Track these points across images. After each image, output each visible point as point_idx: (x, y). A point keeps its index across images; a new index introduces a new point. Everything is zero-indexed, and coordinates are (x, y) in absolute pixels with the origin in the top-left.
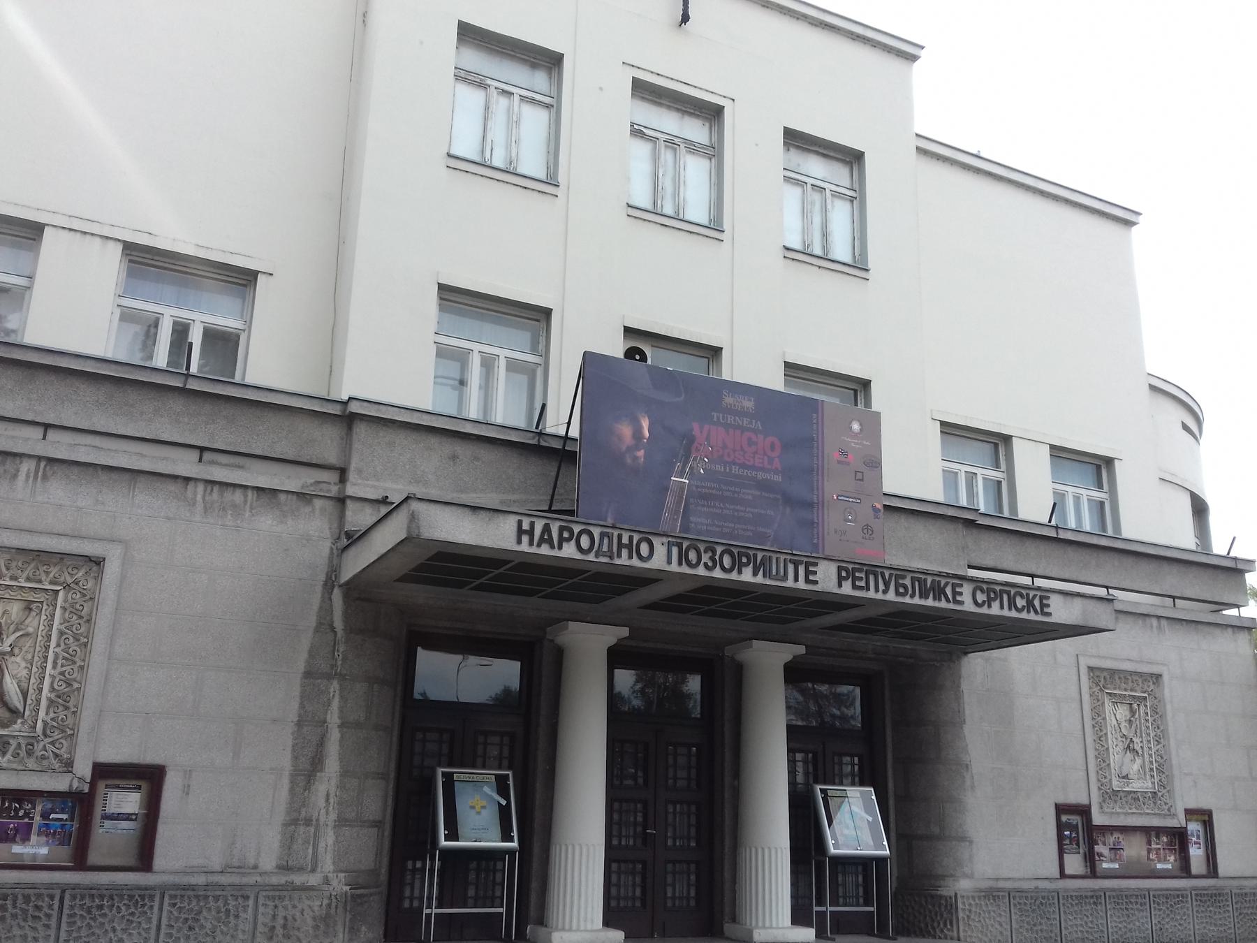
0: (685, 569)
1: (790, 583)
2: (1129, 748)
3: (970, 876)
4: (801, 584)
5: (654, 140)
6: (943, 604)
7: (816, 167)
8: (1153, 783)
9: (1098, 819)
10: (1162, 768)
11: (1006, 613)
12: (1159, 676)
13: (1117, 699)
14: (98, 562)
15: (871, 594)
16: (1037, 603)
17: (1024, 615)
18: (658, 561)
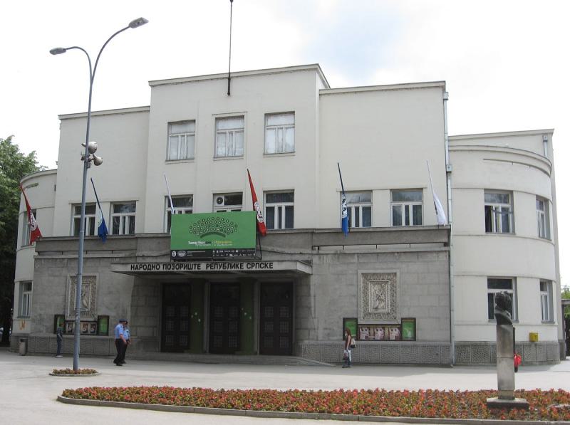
0: (168, 270)
1: (194, 270)
2: (379, 298)
4: (196, 270)
5: (225, 133)
6: (237, 269)
9: (360, 322)
10: (394, 304)
11: (257, 269)
12: (395, 273)
13: (375, 283)
14: (95, 277)
15: (216, 269)
16: (268, 265)
17: (264, 269)
18: (161, 269)
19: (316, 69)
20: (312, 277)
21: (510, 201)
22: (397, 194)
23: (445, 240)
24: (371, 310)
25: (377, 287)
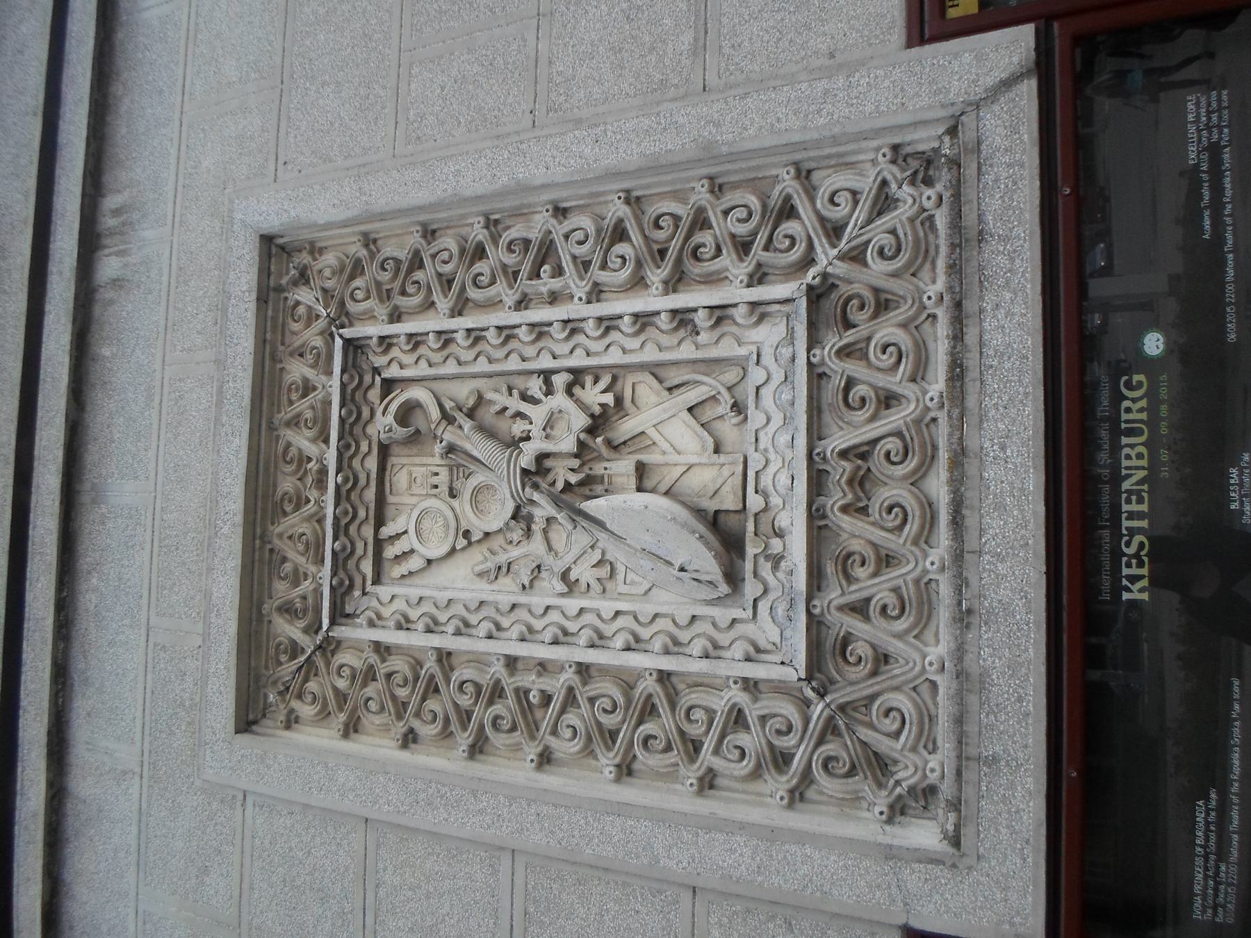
2: (567, 486)
12: (272, 247)
13: (363, 544)
24: (776, 634)
25: (421, 509)
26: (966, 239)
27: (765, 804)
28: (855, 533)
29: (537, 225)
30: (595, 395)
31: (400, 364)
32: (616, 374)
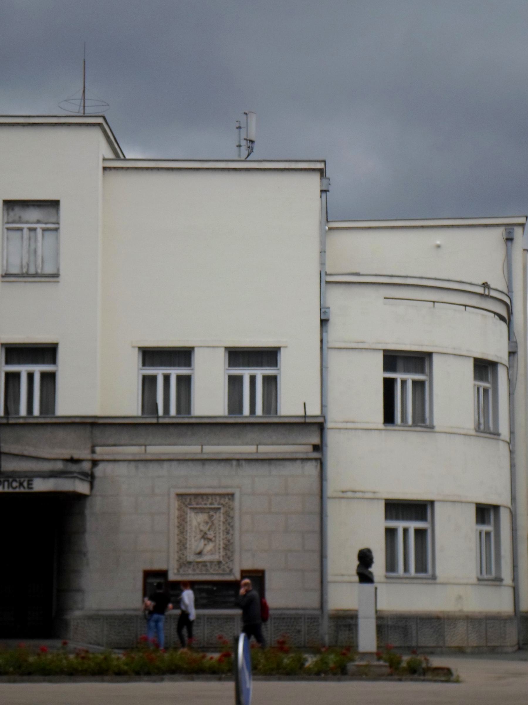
2: (205, 537)
3: (82, 609)
7: (33, 214)
8: (220, 557)
10: (228, 546)
12: (232, 495)
17: (17, 490)
19: (99, 125)
20: (88, 503)
21: (427, 370)
22: (238, 356)
23: (316, 440)
24: (191, 557)
25: (202, 517)
26: (223, 574)
27: (176, 557)
28: (200, 565)
29: (231, 532)
30: (213, 539)
31: (218, 514)
32: (215, 541)
